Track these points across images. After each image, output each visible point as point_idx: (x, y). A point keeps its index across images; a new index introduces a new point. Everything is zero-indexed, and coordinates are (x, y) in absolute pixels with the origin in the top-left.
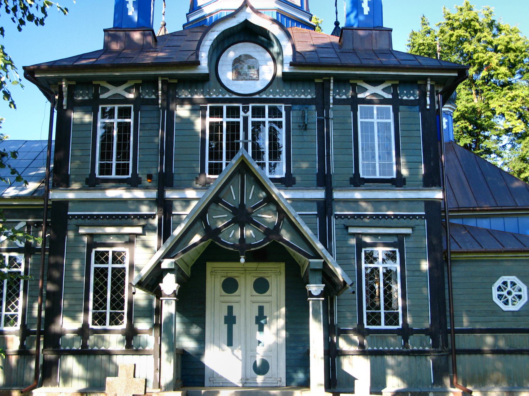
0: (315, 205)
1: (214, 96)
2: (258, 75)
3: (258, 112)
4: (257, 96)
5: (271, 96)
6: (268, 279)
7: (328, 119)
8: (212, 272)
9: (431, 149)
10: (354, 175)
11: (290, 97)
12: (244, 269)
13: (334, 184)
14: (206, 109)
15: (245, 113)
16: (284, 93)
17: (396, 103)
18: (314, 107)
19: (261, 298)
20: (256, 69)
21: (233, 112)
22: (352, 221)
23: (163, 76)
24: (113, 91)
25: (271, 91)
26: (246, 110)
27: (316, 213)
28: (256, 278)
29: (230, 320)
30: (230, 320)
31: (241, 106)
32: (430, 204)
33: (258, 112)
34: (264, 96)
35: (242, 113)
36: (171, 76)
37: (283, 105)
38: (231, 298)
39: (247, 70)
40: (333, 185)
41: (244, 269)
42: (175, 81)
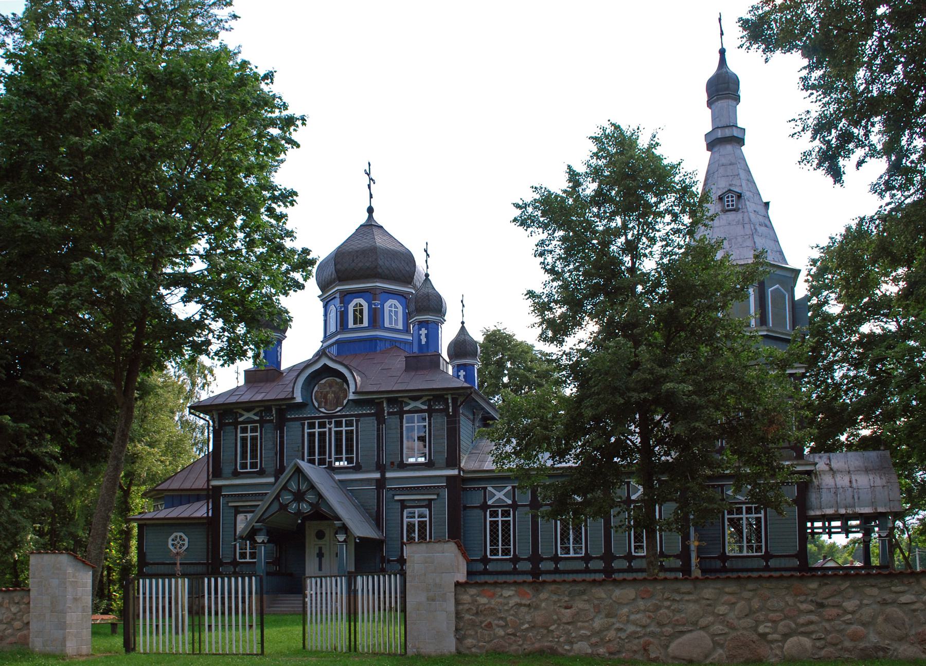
3: (338, 424)
17: (430, 411)
21: (322, 425)
24: (247, 415)
26: (330, 423)
29: (320, 555)
30: (320, 555)
32: (449, 478)
33: (338, 424)
38: (321, 542)
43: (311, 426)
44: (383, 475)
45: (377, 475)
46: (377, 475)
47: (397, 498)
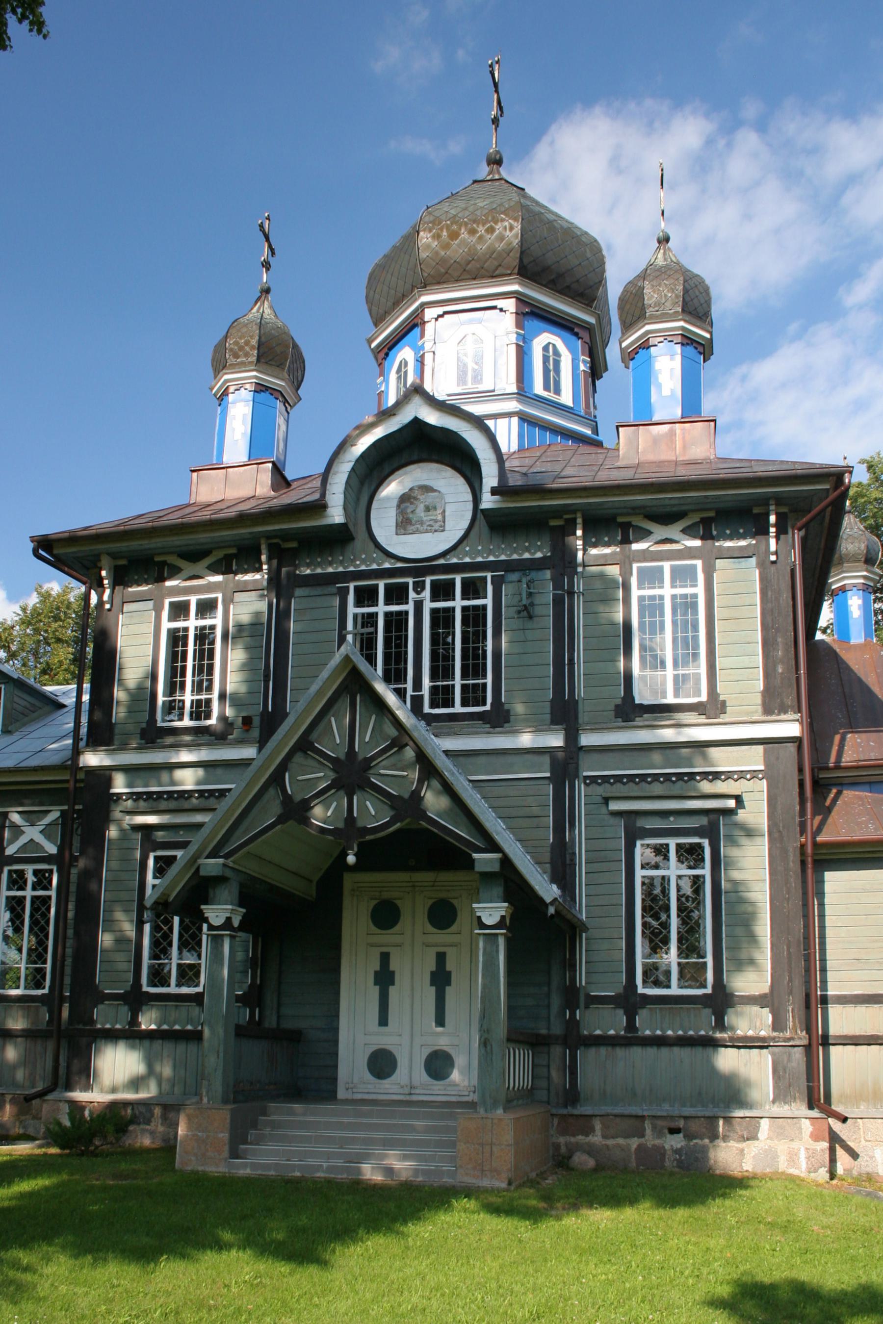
0: (546, 759)
1: (363, 568)
2: (444, 522)
3: (442, 591)
4: (442, 561)
5: (467, 560)
6: (455, 902)
7: (571, 593)
8: (353, 890)
9: (779, 640)
10: (623, 699)
11: (503, 558)
12: (411, 884)
13: (583, 717)
14: (348, 593)
15: (418, 593)
16: (490, 552)
18: (548, 574)
19: (441, 937)
20: (439, 511)
21: (397, 594)
22: (619, 789)
23: (268, 536)
25: (467, 549)
26: (419, 587)
27: (548, 775)
28: (433, 901)
29: (385, 978)
30: (385, 978)
31: (410, 581)
33: (442, 591)
34: (455, 560)
35: (412, 595)
36: (285, 535)
37: (489, 575)
38: (387, 937)
39: (423, 514)
40: (580, 721)
41: (411, 884)
42: (294, 545)
43: (366, 596)
44: (572, 737)
45: (556, 740)
46: (556, 740)
47: (614, 806)
